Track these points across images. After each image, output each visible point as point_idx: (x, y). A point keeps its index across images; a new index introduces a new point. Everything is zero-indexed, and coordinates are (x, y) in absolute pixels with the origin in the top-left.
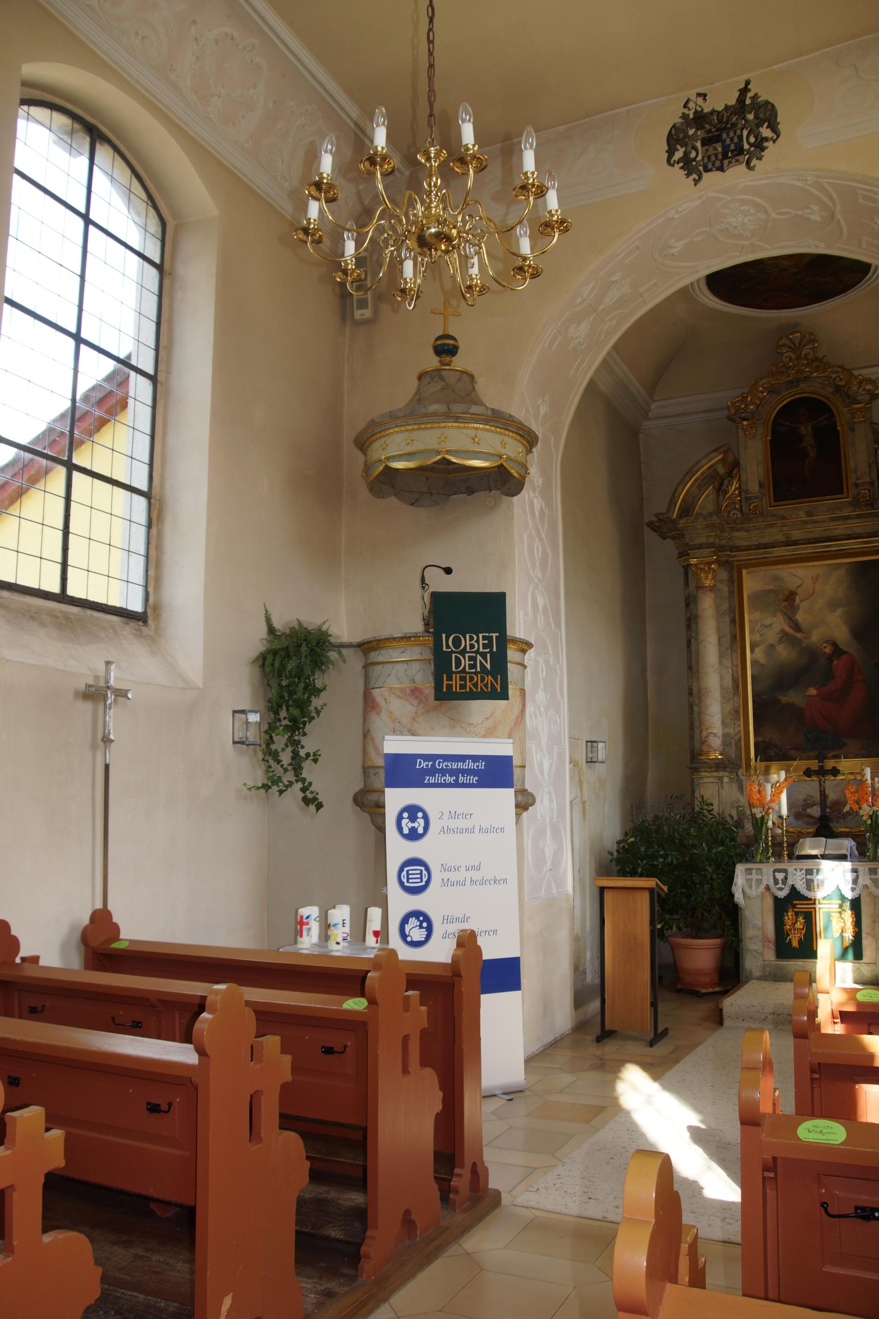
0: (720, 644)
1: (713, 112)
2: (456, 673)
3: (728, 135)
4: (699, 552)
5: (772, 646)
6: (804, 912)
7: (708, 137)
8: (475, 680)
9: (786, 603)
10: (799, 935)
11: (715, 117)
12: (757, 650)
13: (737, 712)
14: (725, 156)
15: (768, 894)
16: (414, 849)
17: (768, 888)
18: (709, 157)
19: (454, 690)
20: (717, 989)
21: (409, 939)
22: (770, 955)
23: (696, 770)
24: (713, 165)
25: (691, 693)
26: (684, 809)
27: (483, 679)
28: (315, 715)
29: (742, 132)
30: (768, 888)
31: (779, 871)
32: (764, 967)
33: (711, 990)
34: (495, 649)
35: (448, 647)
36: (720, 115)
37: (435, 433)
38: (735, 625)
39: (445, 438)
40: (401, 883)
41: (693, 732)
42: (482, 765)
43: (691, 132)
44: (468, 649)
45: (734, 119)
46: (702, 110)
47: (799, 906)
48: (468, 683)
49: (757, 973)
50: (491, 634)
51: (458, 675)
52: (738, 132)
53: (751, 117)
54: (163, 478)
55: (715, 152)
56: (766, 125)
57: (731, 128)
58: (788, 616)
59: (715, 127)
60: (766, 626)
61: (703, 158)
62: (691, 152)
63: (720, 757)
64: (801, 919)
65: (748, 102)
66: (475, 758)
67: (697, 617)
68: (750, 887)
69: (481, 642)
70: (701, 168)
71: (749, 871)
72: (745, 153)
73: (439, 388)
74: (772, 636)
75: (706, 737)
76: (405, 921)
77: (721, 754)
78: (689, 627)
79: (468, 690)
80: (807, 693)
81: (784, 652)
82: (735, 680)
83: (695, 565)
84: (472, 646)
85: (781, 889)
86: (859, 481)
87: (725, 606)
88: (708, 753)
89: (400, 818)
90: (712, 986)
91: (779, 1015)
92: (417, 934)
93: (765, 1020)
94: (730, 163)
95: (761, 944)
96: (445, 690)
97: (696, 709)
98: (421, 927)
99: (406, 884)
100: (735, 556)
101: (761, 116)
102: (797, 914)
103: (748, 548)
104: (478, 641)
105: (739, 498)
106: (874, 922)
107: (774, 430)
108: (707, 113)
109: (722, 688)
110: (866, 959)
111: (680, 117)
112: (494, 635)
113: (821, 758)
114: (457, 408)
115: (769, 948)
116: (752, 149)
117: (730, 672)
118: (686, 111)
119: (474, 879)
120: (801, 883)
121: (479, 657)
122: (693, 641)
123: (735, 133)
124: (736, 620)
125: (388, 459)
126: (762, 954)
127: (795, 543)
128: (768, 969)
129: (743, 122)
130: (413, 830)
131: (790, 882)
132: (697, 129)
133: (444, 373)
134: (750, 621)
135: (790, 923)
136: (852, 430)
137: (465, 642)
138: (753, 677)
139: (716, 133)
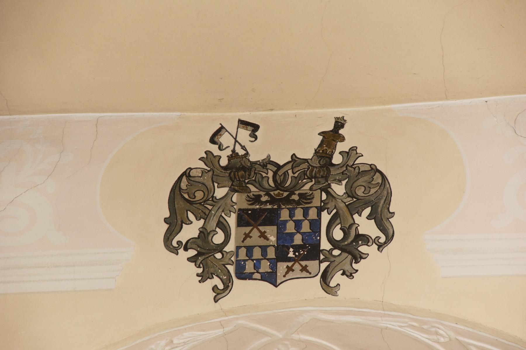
1: (267, 163)
3: (291, 215)
7: (253, 210)
11: (270, 174)
14: (281, 256)
18: (250, 250)
24: (257, 267)
29: (319, 215)
36: (280, 172)
43: (220, 193)
45: (307, 187)
46: (247, 154)
52: (313, 214)
53: (339, 189)
55: (262, 242)
56: (367, 211)
57: (298, 203)
59: (268, 194)
61: (238, 248)
62: (215, 233)
65: (337, 159)
70: (231, 269)
72: (322, 257)
94: (290, 269)
101: (360, 192)
108: (255, 163)
111: (201, 159)
116: (336, 252)
118: (214, 149)
123: (306, 214)
129: (324, 196)
132: (233, 190)
139: (269, 206)
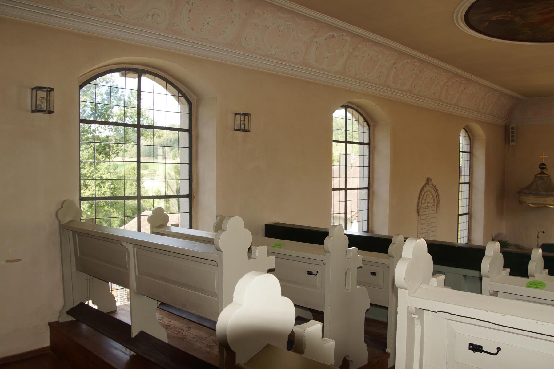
54: (471, 207)
114: (549, 193)
125: (529, 203)
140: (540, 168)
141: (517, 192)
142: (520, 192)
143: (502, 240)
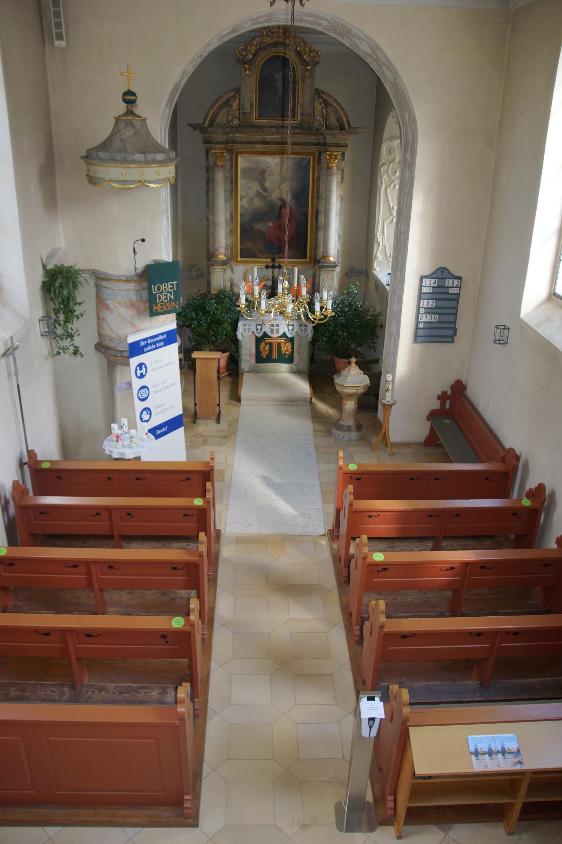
0: (225, 196)
2: (159, 303)
4: (217, 146)
5: (251, 199)
6: (269, 343)
8: (167, 305)
9: (260, 176)
10: (266, 353)
12: (244, 200)
13: (231, 231)
15: (253, 334)
16: (143, 382)
17: (253, 332)
19: (158, 311)
20: (226, 374)
21: (143, 420)
22: (253, 361)
23: (213, 265)
25: (208, 220)
26: (197, 271)
27: (170, 304)
28: (80, 316)
30: (253, 332)
31: (259, 325)
32: (250, 367)
33: (224, 375)
34: (175, 289)
35: (155, 291)
37: (139, 170)
38: (233, 185)
39: (144, 173)
40: (139, 398)
41: (209, 241)
42: (165, 336)
44: (164, 291)
47: (266, 340)
48: (164, 307)
49: (247, 369)
50: (173, 282)
51: (160, 304)
58: (260, 183)
60: (249, 188)
63: (224, 258)
64: (268, 346)
66: (162, 334)
67: (213, 179)
68: (245, 332)
69: (169, 286)
71: (245, 325)
73: (133, 133)
74: (252, 193)
75: (217, 247)
76: (142, 413)
77: (224, 256)
78: (208, 183)
79: (164, 310)
80: (268, 225)
81: (258, 203)
82: (231, 215)
83: (215, 153)
84: (165, 289)
85: (259, 333)
86: (304, 113)
87: (228, 174)
88: (218, 255)
89: (136, 370)
90: (224, 373)
91: (265, 398)
92: (146, 417)
93: (259, 400)
95: (249, 357)
96: (154, 311)
97: (211, 229)
98: (148, 414)
99: (141, 398)
100: (235, 146)
102: (266, 344)
103: (242, 143)
104: (168, 287)
105: (238, 111)
106: (299, 347)
107: (261, 73)
109: (226, 220)
110: (295, 362)
112: (175, 282)
113: (273, 260)
114: (150, 157)
115: (252, 358)
117: (229, 210)
119: (165, 387)
120: (268, 330)
121: (169, 294)
122: (210, 192)
124: (233, 182)
125: (110, 181)
126: (249, 361)
127: (267, 143)
128: (252, 367)
130: (142, 374)
131: (264, 330)
133: (134, 122)
134: (241, 184)
135: (263, 348)
136: (303, 80)
137: (162, 288)
138: (241, 215)
140: (125, 101)
141: (82, 157)
142: (88, 157)
143: (62, 265)
